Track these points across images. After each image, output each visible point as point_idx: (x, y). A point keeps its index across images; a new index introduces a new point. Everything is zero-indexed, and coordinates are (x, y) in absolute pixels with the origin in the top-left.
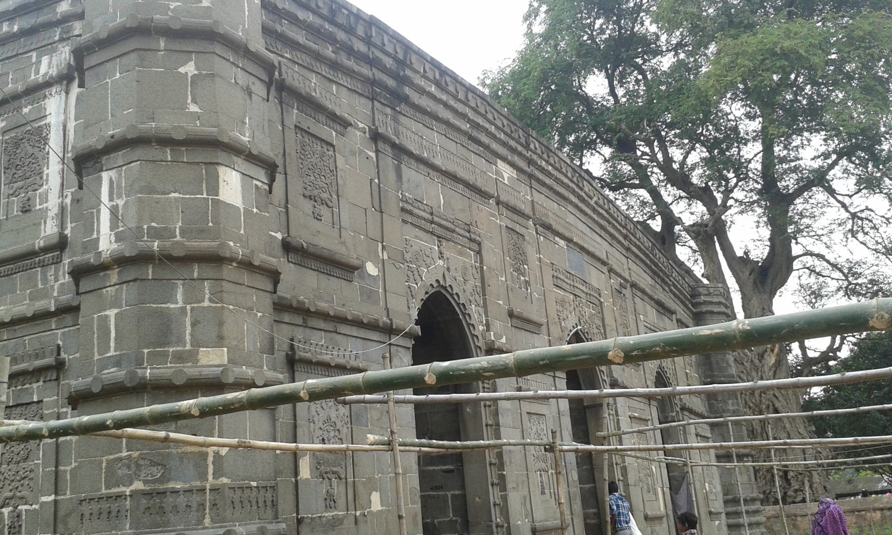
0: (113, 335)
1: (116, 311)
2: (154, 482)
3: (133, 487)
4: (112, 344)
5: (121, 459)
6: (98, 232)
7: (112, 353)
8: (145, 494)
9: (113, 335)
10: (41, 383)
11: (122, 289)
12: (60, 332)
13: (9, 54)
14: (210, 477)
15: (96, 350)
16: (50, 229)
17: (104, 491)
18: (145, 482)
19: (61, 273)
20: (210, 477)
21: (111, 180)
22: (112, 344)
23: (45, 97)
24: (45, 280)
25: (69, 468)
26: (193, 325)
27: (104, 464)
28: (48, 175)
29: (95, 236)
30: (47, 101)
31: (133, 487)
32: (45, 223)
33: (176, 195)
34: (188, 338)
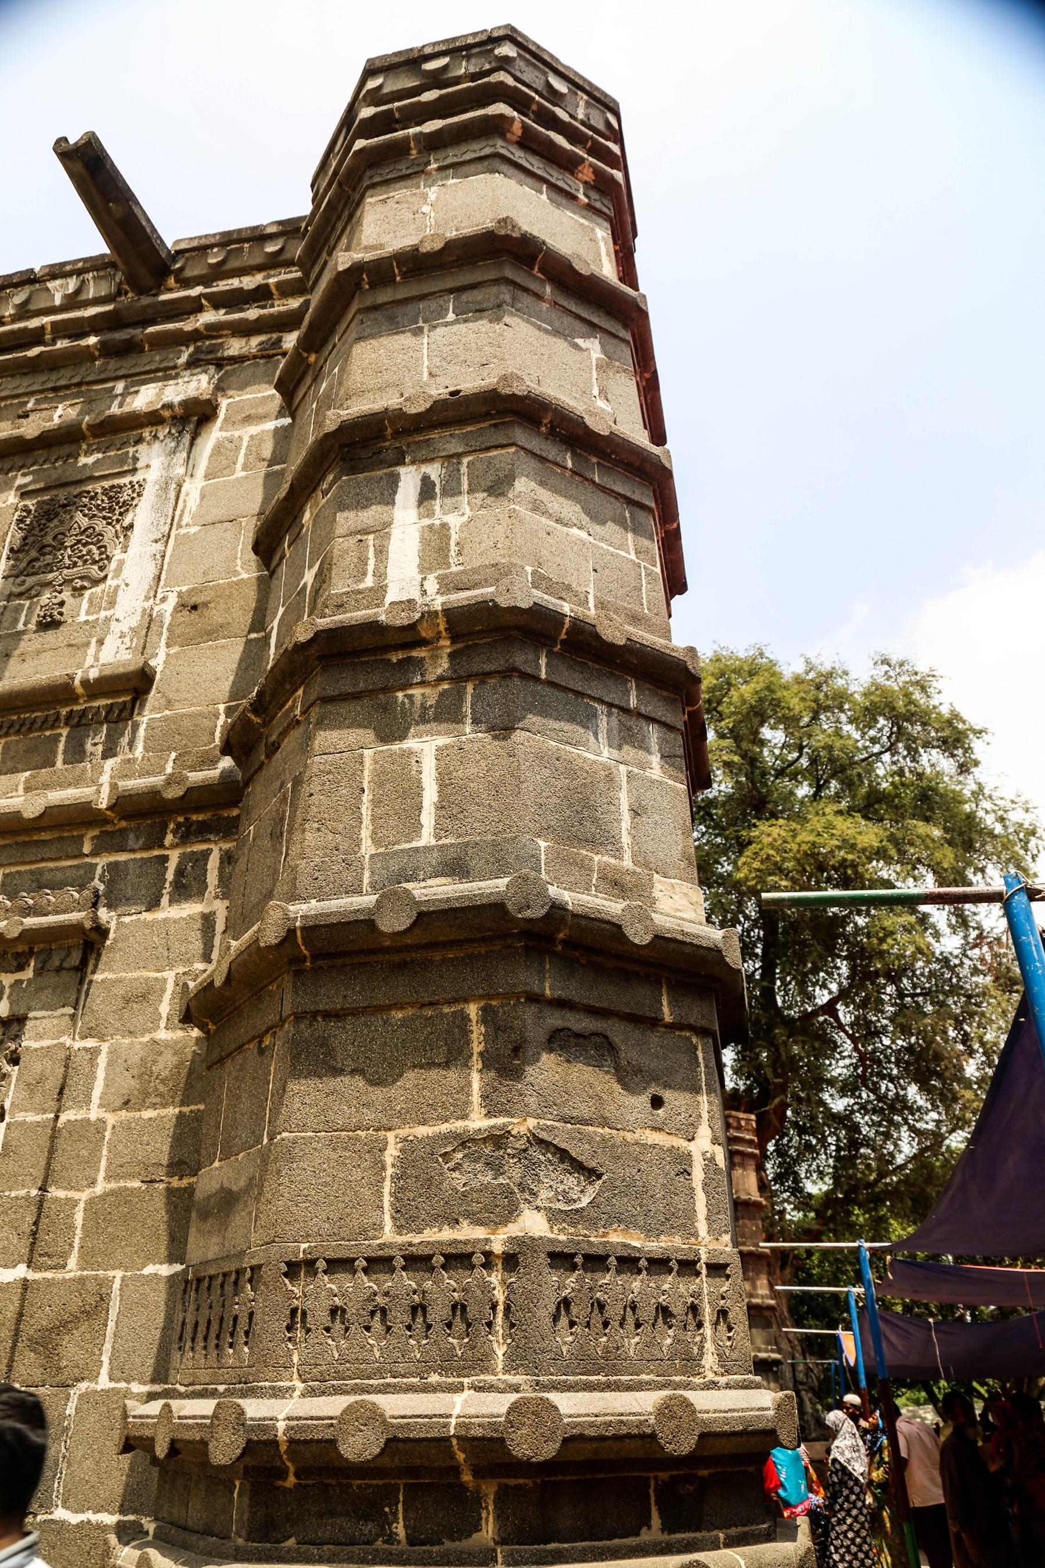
0: (430, 795)
1: (442, 741)
2: (575, 1217)
3: (513, 1230)
4: (428, 818)
5: (464, 1141)
6: (380, 575)
7: (427, 838)
8: (561, 1259)
9: (430, 795)
10: (29, 973)
11: (461, 695)
12: (101, 862)
13: (63, 382)
14: (702, 1227)
15: (365, 833)
16: (113, 655)
17: (389, 1234)
18: (554, 1217)
19: (125, 740)
20: (702, 1227)
21: (426, 481)
22: (428, 818)
23: (139, 440)
24: (76, 753)
25: (84, 1196)
26: (635, 813)
27: (391, 1153)
28: (122, 563)
29: (369, 582)
30: (142, 448)
31: (513, 1230)
32: (101, 642)
33: (583, 535)
34: (626, 839)
